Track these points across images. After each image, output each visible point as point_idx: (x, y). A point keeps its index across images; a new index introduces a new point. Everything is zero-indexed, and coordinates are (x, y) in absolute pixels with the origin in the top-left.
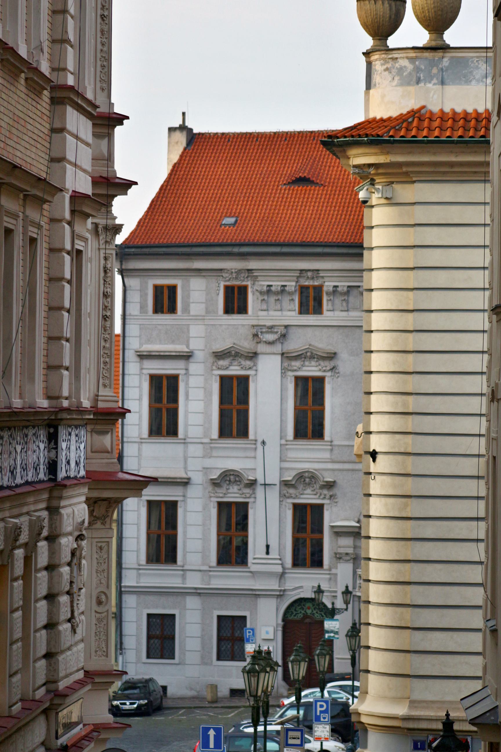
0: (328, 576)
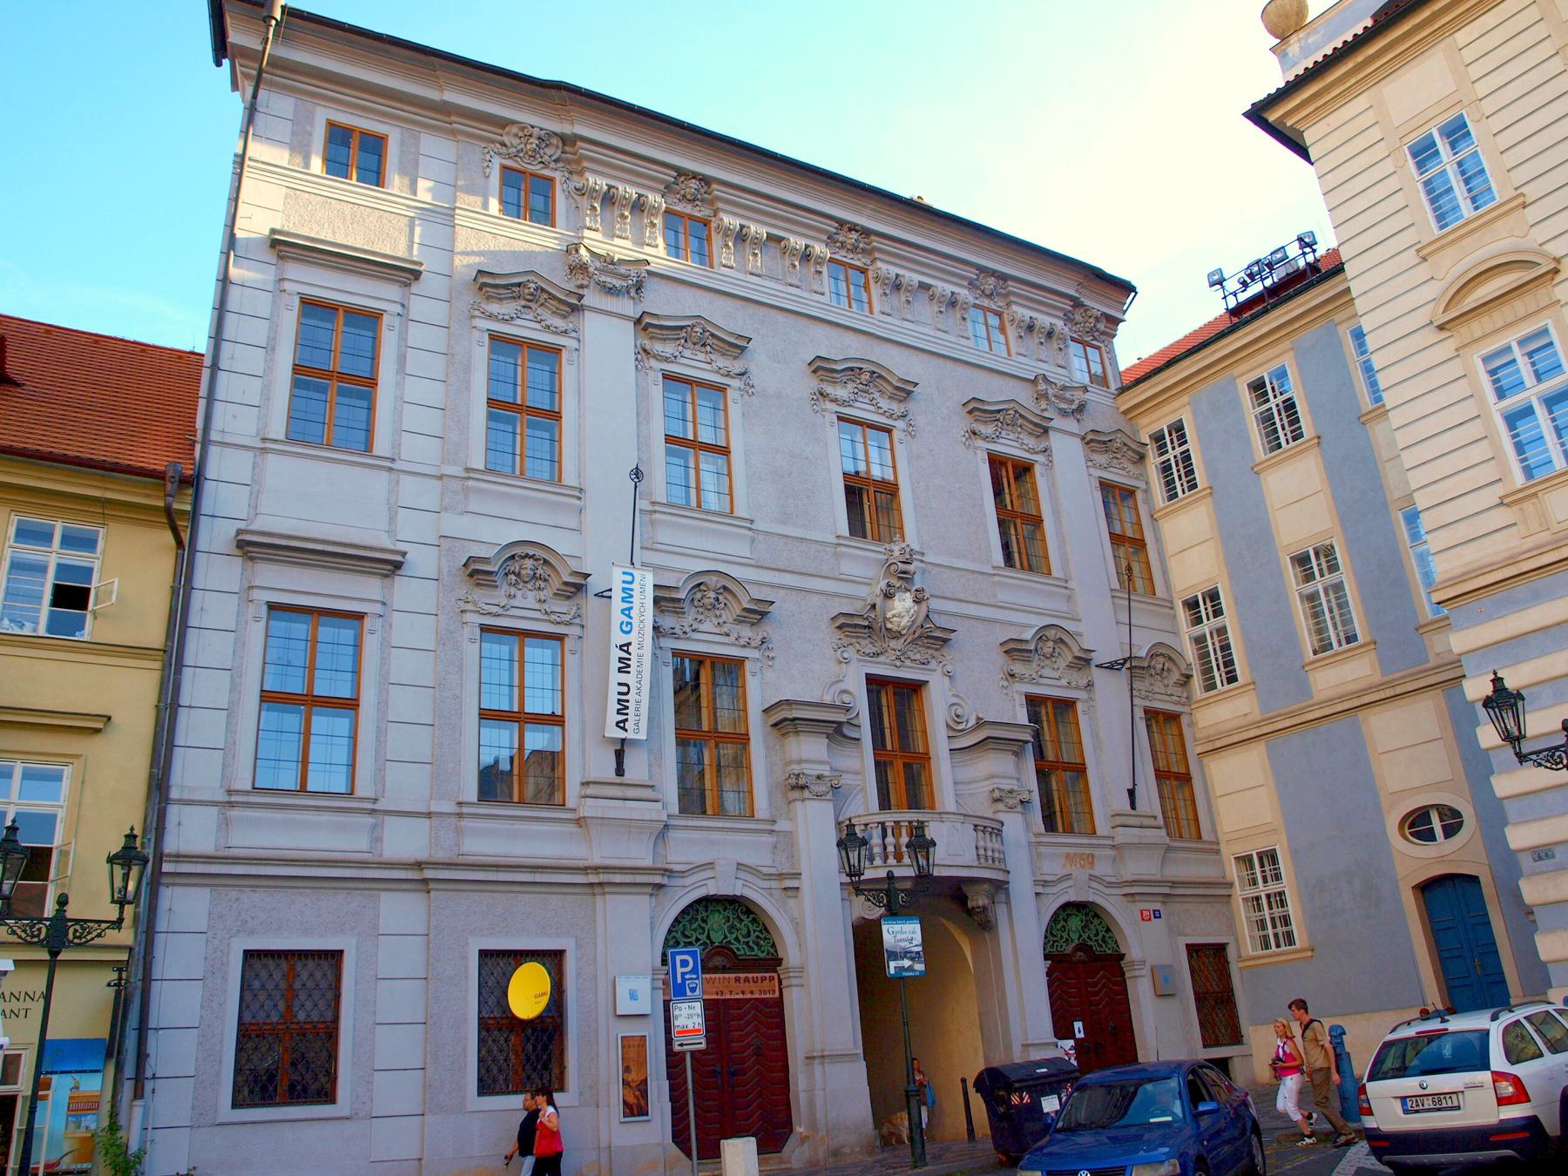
0: (771, 839)
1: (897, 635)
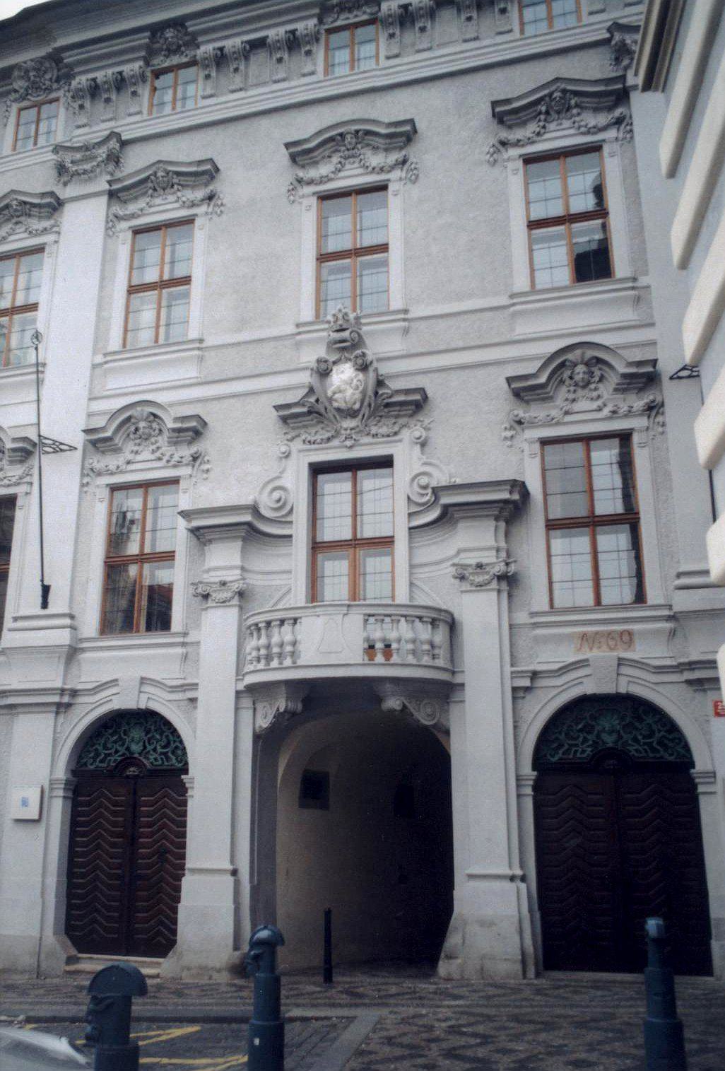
1: (352, 413)
